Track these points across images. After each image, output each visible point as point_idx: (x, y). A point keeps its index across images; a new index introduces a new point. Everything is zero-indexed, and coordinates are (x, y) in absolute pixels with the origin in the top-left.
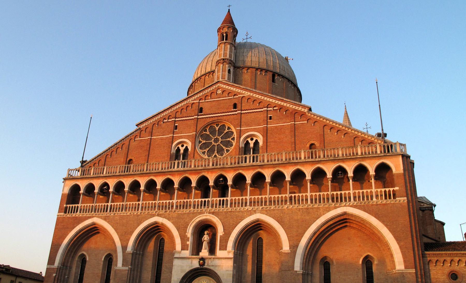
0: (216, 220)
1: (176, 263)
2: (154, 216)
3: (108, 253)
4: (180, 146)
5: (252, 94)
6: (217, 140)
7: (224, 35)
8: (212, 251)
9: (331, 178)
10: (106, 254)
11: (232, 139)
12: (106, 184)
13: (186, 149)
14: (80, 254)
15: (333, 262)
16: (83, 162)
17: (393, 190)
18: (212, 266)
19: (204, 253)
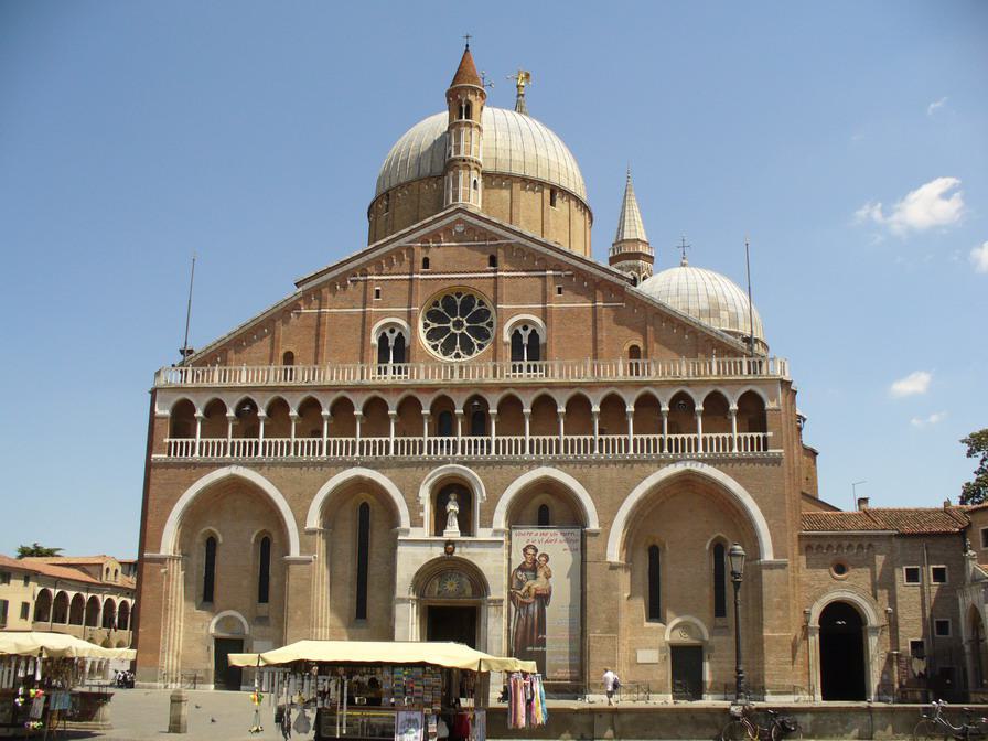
0: (472, 473)
1: (401, 549)
2: (352, 465)
3: (262, 529)
4: (387, 332)
5: (523, 241)
6: (458, 325)
7: (464, 106)
8: (466, 527)
9: (669, 412)
10: (257, 532)
11: (488, 325)
12: (248, 401)
13: (400, 338)
14: (203, 531)
15: (664, 547)
16: (186, 352)
17: (765, 438)
18: (468, 554)
19: (452, 531)
